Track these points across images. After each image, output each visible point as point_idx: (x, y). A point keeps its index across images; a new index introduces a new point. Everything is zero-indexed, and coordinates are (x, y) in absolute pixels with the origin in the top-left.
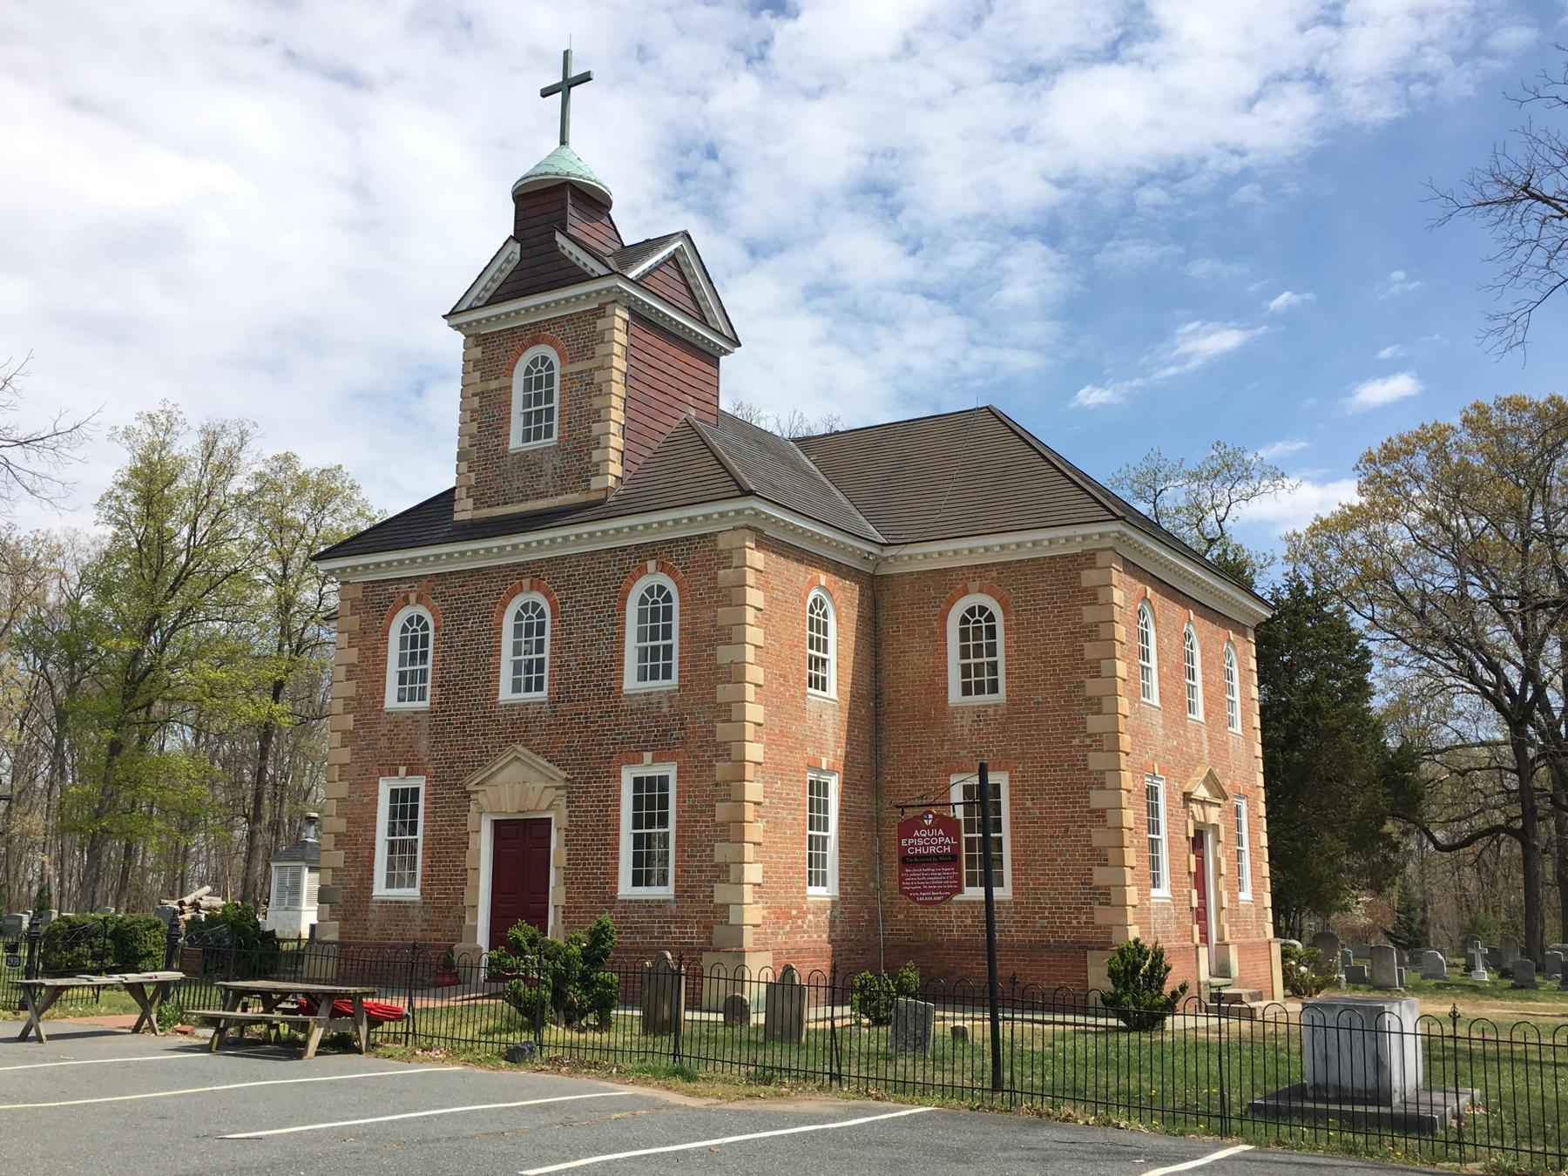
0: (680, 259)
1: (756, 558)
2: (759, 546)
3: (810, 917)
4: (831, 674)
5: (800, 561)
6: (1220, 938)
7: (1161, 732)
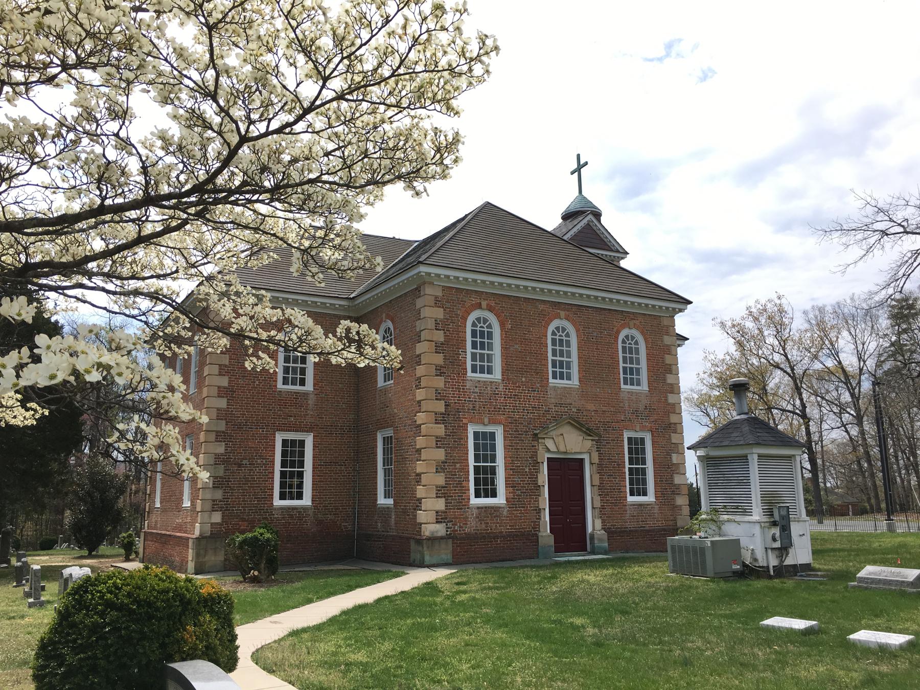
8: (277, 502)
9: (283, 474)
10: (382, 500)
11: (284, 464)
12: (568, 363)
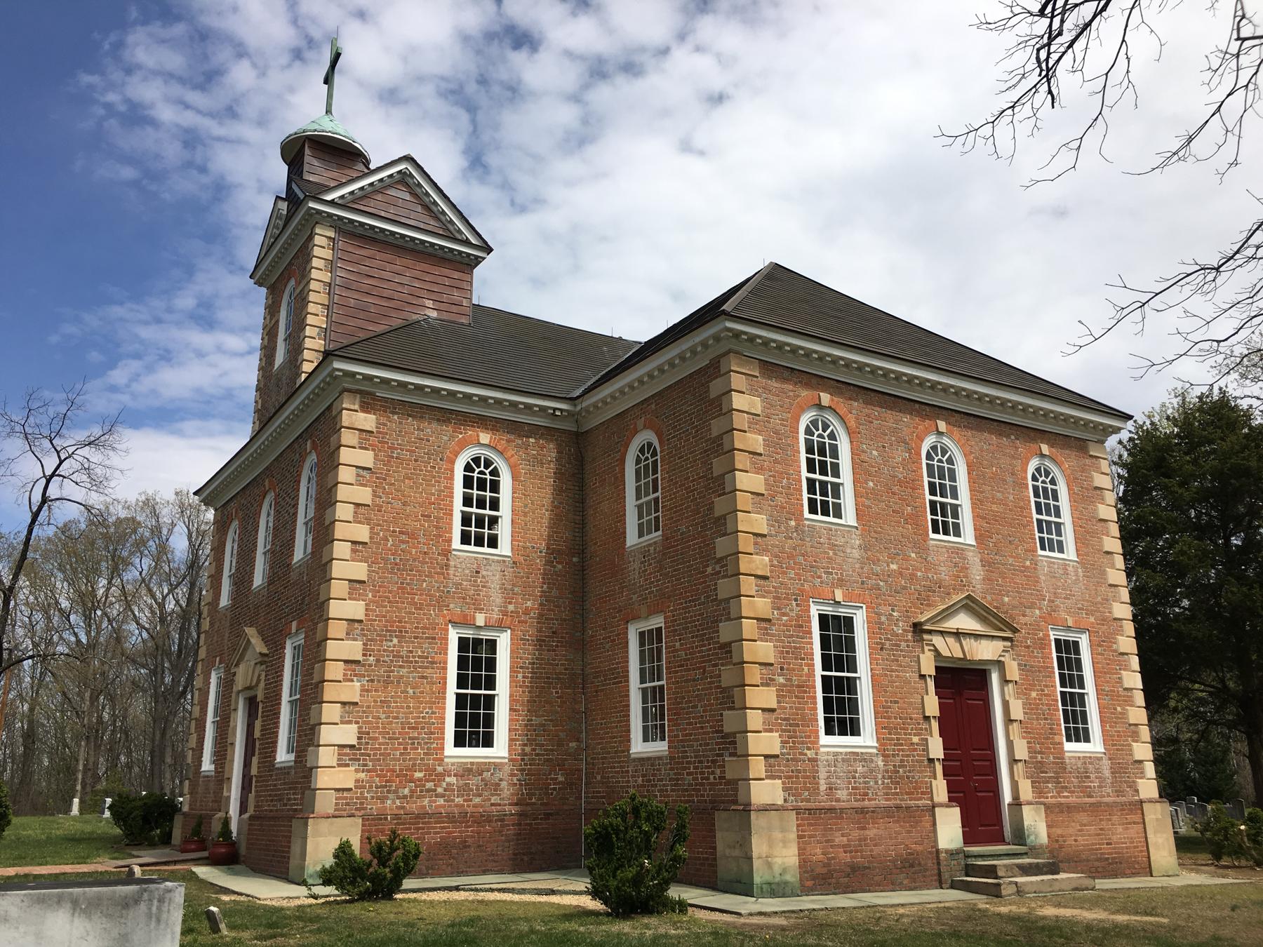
0: (410, 181)
1: (355, 418)
2: (365, 408)
3: (453, 780)
4: (504, 531)
5: (447, 421)
6: (1016, 796)
7: (856, 554)
8: (450, 750)
9: (461, 700)
10: (638, 746)
11: (461, 683)
12: (955, 509)
